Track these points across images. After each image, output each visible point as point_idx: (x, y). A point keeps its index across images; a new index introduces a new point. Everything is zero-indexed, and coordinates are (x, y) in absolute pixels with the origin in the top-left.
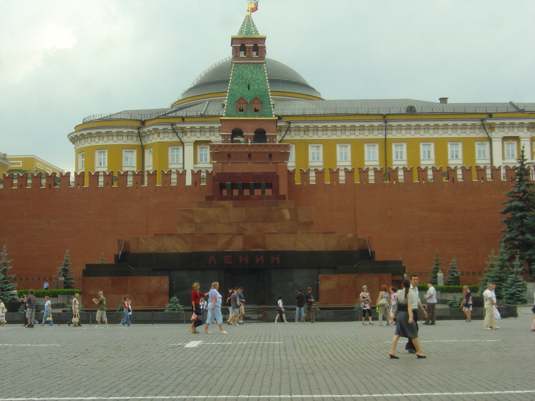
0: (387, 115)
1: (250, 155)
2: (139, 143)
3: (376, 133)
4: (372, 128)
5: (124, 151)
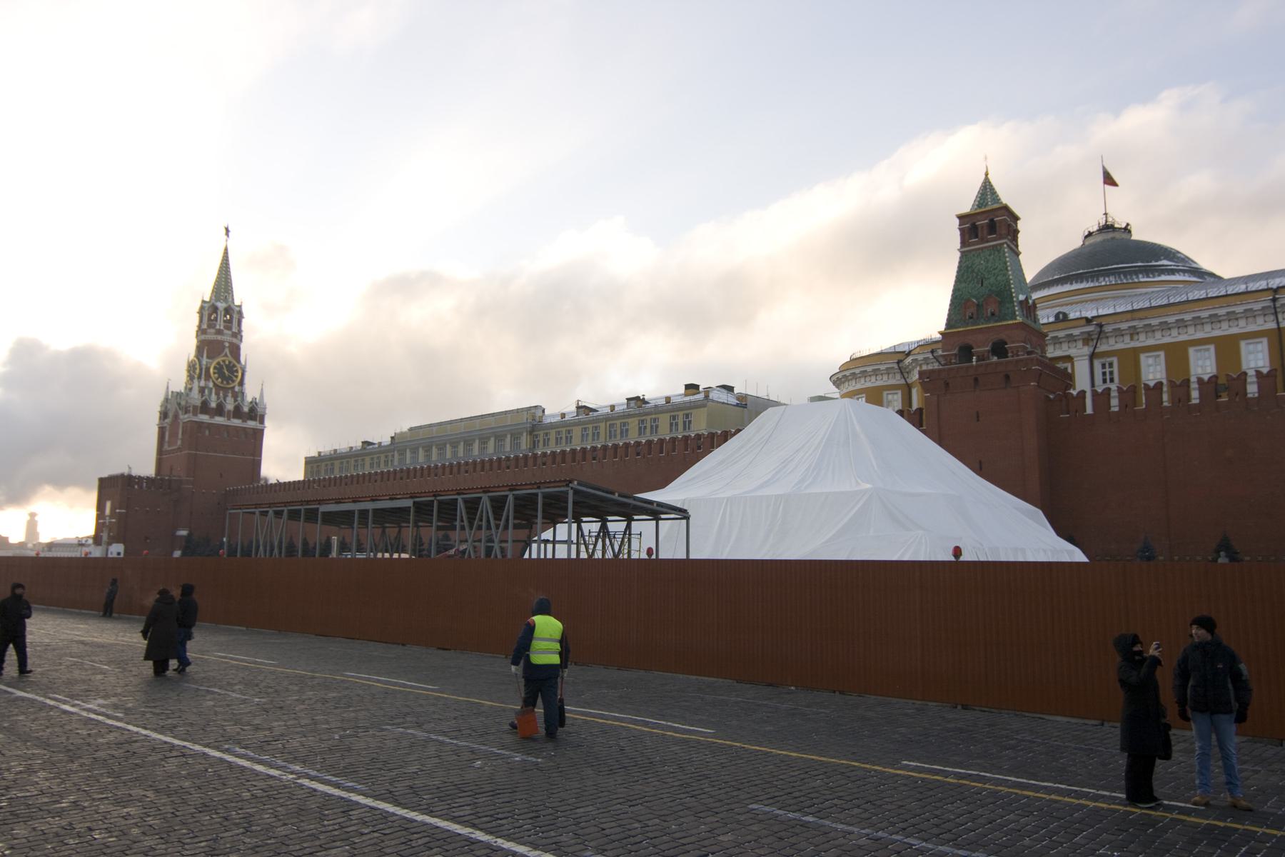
0: (1278, 288)
1: (976, 380)
2: (903, 382)
3: (1260, 320)
4: (1250, 315)
5: (885, 393)
